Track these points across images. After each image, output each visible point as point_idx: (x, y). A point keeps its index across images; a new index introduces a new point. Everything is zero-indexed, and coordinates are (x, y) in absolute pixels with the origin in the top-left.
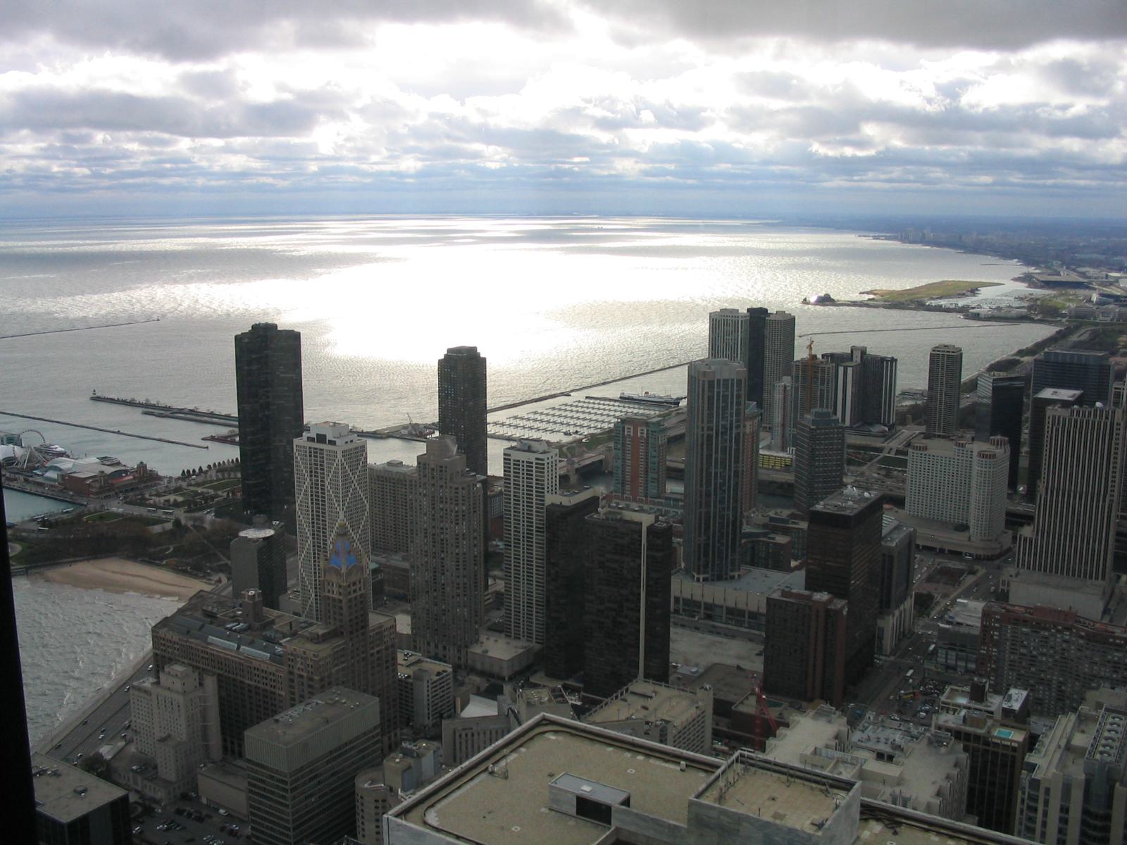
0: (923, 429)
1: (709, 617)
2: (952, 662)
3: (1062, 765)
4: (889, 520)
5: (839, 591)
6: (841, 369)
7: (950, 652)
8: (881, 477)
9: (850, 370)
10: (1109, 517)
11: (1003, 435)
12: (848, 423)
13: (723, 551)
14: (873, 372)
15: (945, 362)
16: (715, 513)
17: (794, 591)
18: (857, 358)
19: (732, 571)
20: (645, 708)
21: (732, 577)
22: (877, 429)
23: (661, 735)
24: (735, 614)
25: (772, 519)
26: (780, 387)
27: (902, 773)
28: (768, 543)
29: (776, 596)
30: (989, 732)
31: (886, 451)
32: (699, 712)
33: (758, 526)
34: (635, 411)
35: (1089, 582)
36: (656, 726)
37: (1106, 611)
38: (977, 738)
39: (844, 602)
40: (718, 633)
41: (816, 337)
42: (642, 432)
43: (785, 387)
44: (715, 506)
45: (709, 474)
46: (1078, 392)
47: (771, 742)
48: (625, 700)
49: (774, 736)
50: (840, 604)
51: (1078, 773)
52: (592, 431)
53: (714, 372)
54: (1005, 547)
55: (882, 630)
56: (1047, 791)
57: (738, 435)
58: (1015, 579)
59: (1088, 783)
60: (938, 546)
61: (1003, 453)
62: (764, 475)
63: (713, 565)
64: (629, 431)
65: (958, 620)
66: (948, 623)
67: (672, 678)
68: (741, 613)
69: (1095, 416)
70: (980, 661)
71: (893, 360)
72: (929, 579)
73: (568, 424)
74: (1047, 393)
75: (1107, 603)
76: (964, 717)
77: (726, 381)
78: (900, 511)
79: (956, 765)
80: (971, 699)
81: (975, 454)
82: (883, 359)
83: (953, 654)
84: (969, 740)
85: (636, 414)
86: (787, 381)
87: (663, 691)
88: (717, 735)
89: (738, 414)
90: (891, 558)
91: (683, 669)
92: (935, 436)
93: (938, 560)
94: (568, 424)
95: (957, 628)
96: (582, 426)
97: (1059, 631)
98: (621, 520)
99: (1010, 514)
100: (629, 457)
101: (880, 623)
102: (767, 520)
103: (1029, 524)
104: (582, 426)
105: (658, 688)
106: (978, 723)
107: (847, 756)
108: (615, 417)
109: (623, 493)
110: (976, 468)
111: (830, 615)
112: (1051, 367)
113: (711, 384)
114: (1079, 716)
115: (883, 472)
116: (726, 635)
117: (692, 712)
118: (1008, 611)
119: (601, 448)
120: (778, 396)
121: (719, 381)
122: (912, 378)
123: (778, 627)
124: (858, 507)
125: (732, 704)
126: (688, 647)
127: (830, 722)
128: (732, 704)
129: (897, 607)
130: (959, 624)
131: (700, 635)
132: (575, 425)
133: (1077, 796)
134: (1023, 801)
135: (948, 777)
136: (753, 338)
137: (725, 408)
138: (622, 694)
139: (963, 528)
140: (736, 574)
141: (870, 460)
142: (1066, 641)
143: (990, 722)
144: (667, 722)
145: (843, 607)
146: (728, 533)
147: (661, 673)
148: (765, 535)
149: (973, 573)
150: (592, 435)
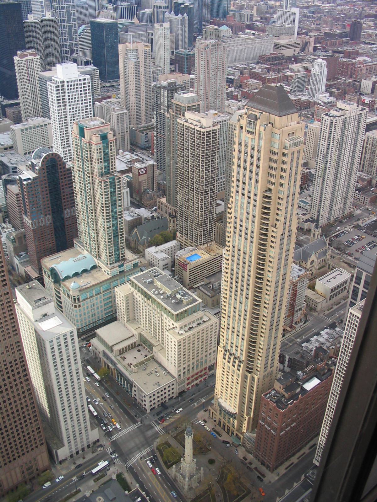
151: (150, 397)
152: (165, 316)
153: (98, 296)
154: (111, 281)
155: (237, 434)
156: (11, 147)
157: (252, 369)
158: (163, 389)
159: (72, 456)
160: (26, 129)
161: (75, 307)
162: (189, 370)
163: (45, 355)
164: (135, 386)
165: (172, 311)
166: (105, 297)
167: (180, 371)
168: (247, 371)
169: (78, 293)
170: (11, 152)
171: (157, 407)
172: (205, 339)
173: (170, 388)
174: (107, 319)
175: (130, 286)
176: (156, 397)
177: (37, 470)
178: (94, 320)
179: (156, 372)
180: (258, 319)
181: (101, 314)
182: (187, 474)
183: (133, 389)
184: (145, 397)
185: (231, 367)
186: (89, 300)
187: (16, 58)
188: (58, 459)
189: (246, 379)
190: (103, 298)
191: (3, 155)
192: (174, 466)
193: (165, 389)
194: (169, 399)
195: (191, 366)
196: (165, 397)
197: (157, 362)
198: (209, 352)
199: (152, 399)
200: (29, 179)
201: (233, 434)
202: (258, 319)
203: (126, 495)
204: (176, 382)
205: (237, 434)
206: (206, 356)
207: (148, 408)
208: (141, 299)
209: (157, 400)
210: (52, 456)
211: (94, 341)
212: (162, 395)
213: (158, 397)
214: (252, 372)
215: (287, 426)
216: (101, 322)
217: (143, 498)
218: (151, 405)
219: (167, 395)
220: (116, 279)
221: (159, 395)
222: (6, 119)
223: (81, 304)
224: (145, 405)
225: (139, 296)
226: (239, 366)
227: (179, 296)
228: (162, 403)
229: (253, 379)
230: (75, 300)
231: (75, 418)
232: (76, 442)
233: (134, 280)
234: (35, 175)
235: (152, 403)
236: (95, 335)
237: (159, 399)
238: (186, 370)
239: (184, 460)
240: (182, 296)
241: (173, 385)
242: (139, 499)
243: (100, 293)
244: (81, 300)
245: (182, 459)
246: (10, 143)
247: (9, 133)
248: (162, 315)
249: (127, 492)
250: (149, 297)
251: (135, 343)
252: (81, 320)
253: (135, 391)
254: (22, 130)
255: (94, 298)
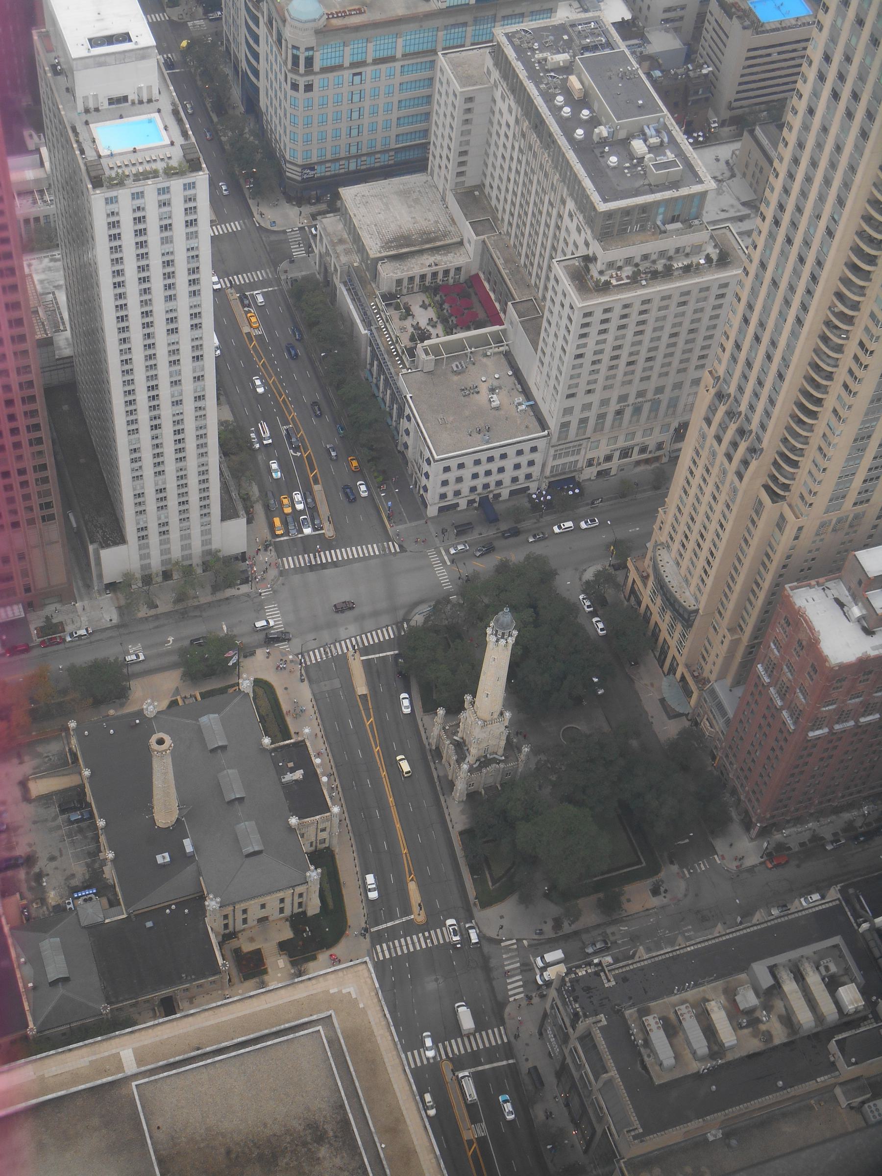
151: (447, 469)
152: (571, 205)
153: (383, 67)
154: (439, 22)
155: (683, 678)
157: (786, 487)
158: (496, 454)
159: (147, 580)
161: (295, 87)
162: (602, 417)
163: (90, 239)
164: (409, 419)
165: (595, 197)
166: (407, 78)
167: (568, 411)
168: (767, 487)
169: (312, 41)
171: (463, 504)
172: (687, 325)
173: (523, 460)
174: (402, 157)
175: (489, 62)
176: (467, 473)
177: (28, 590)
178: (354, 150)
179: (492, 390)
180: (850, 320)
181: (381, 129)
182: (474, 752)
183: (404, 424)
184: (429, 463)
185: (721, 458)
186: (347, 74)
188: (100, 576)
189: (758, 513)
190: (398, 79)
192: (441, 711)
193: (504, 456)
194: (512, 493)
195: (614, 407)
196: (499, 483)
197: (508, 356)
198: (692, 374)
199: (451, 476)
201: (672, 670)
202: (850, 320)
203: (263, 750)
204: (550, 445)
205: (683, 678)
206: (678, 386)
207: (432, 497)
208: (512, 122)
209: (467, 484)
210: (82, 565)
211: (330, 223)
212: (488, 473)
213: (475, 476)
214: (783, 498)
215: (842, 716)
216: (384, 160)
217: (311, 775)
218: (443, 496)
219: (506, 477)
220: (461, 19)
221: (481, 470)
223: (317, 81)
224: (426, 489)
225: (506, 109)
226: (746, 463)
227: (638, 146)
228: (484, 501)
229: (781, 522)
230: (296, 60)
231: (170, 467)
232: (168, 541)
233: (504, 40)
235: (449, 490)
236: (335, 206)
237: (479, 483)
238: (592, 415)
239: (473, 703)
240: (651, 149)
241: (534, 449)
242: (299, 775)
243: (392, 59)
244: (317, 67)
245: (468, 698)
248: (563, 202)
249: (266, 741)
250: (539, 125)
251: (458, 269)
252: (307, 141)
253: (407, 432)
255: (368, 71)
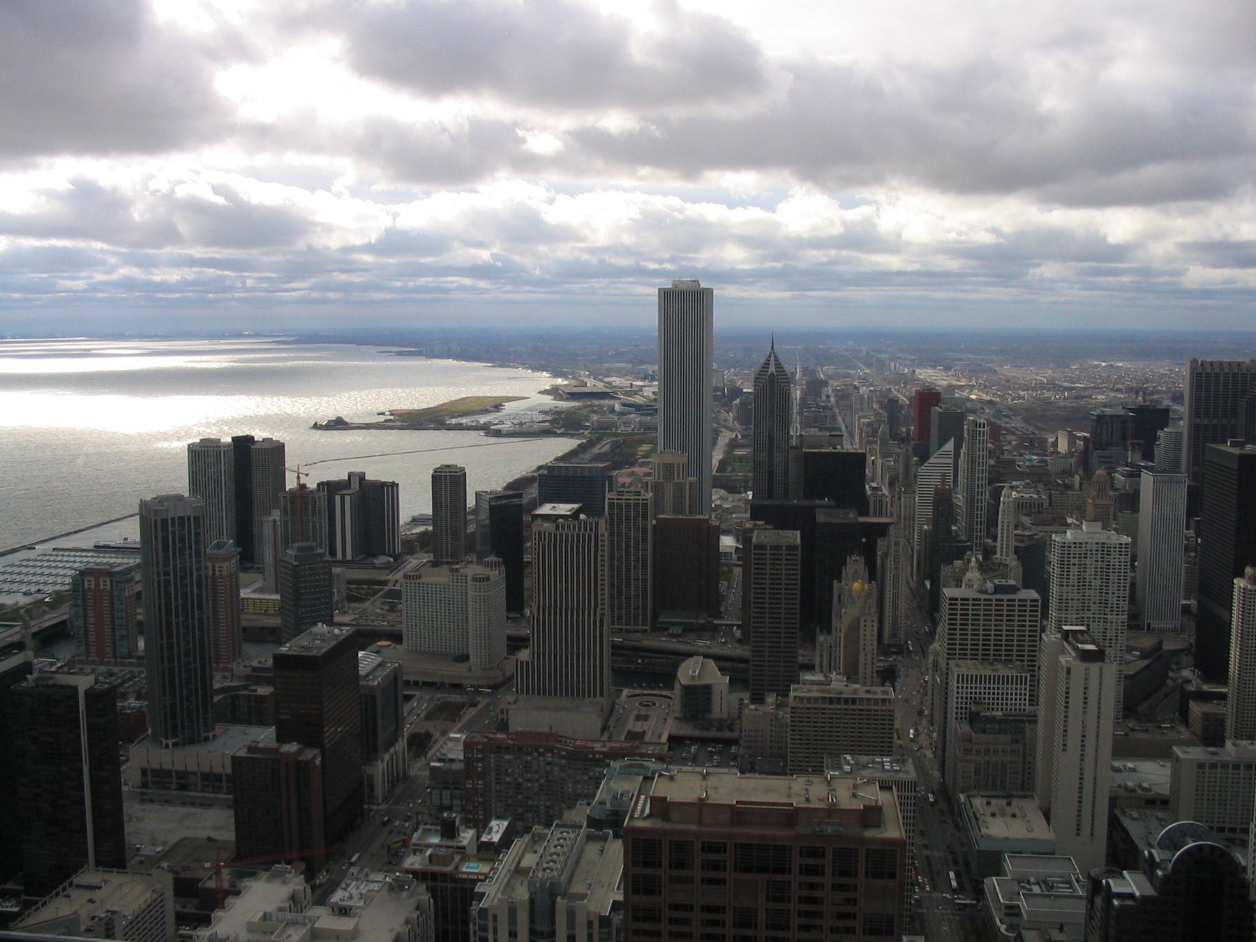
0: (430, 557)
1: (182, 787)
2: (446, 802)
3: (509, 887)
4: (366, 659)
5: (311, 737)
6: (338, 498)
7: (444, 792)
8: (385, 612)
9: (347, 499)
10: (601, 633)
11: (498, 556)
12: (349, 557)
13: (187, 713)
14: (374, 499)
15: (448, 483)
16: (180, 668)
17: (261, 745)
18: (355, 485)
19: (206, 731)
20: (91, 901)
21: (206, 739)
22: (381, 560)
23: (107, 930)
24: (211, 780)
25: (255, 669)
26: (271, 521)
27: (357, 925)
28: (249, 696)
29: (242, 753)
30: (457, 868)
31: (391, 584)
32: (155, 896)
33: (240, 678)
34: (99, 560)
35: (587, 700)
36: (100, 919)
37: (605, 728)
38: (444, 876)
39: (316, 751)
40: (192, 804)
41: (312, 463)
42: (105, 584)
43: (275, 521)
44: (179, 660)
45: (169, 624)
46: (576, 506)
47: (217, 914)
48: (68, 896)
49: (223, 907)
50: (310, 753)
51: (522, 893)
52: (58, 588)
53: (167, 510)
54: (508, 674)
55: (371, 778)
56: (495, 917)
57: (199, 577)
58: (512, 706)
59: (532, 901)
60: (437, 680)
61: (497, 575)
62: (247, 620)
63: (183, 728)
64: (89, 583)
65: (451, 756)
66: (440, 760)
67: (132, 863)
68: (168, 774)
69: (580, 529)
70: (464, 796)
71: (394, 485)
72: (428, 717)
73: (29, 583)
74: (546, 509)
75: (607, 720)
76: (431, 856)
77: (181, 519)
78: (398, 647)
79: (418, 908)
80: (442, 836)
81: (469, 578)
82: (383, 484)
83: (446, 793)
84: (436, 880)
85: (97, 564)
86: (276, 515)
87: (115, 878)
88: (181, 919)
89: (198, 554)
90: (374, 698)
91: (147, 851)
92: (442, 563)
93: (438, 696)
94: (29, 583)
95: (448, 765)
96: (45, 583)
97: (540, 754)
98: (54, 685)
99: (509, 638)
100: (91, 613)
101: (369, 770)
102: (249, 671)
103: (526, 647)
104: (45, 583)
105: (107, 876)
106: (445, 860)
107: (300, 916)
108: (71, 568)
109: (88, 656)
110: (470, 593)
111: (302, 768)
112: (553, 482)
113: (165, 522)
114: (533, 837)
115: (387, 607)
116: (202, 805)
117: (148, 896)
118: (490, 739)
119: (65, 607)
120: (267, 532)
121: (173, 519)
122: (415, 503)
123: (245, 784)
124: (326, 647)
125: (200, 880)
126: (152, 826)
127: (284, 883)
128: (200, 880)
129: (387, 750)
130: (452, 760)
131: (171, 809)
132: (38, 583)
133: (523, 917)
134: (475, 933)
135: (407, 922)
136: (239, 469)
137: (182, 549)
138: (64, 889)
139: (465, 658)
140: (211, 734)
141: (374, 595)
142: (549, 764)
143: (457, 858)
144: (114, 912)
145: (315, 757)
146: (196, 689)
147: (115, 857)
148: (245, 688)
149: (474, 705)
150: (57, 593)
156: (1164, 802)
160: (1213, 766)
170: (1160, 815)
187: (1239, 583)
191: (1135, 814)
200: (1132, 896)
222: (1182, 729)
234: (1150, 891)
246: (1165, 790)
247: (1169, 765)
254: (1201, 766)
